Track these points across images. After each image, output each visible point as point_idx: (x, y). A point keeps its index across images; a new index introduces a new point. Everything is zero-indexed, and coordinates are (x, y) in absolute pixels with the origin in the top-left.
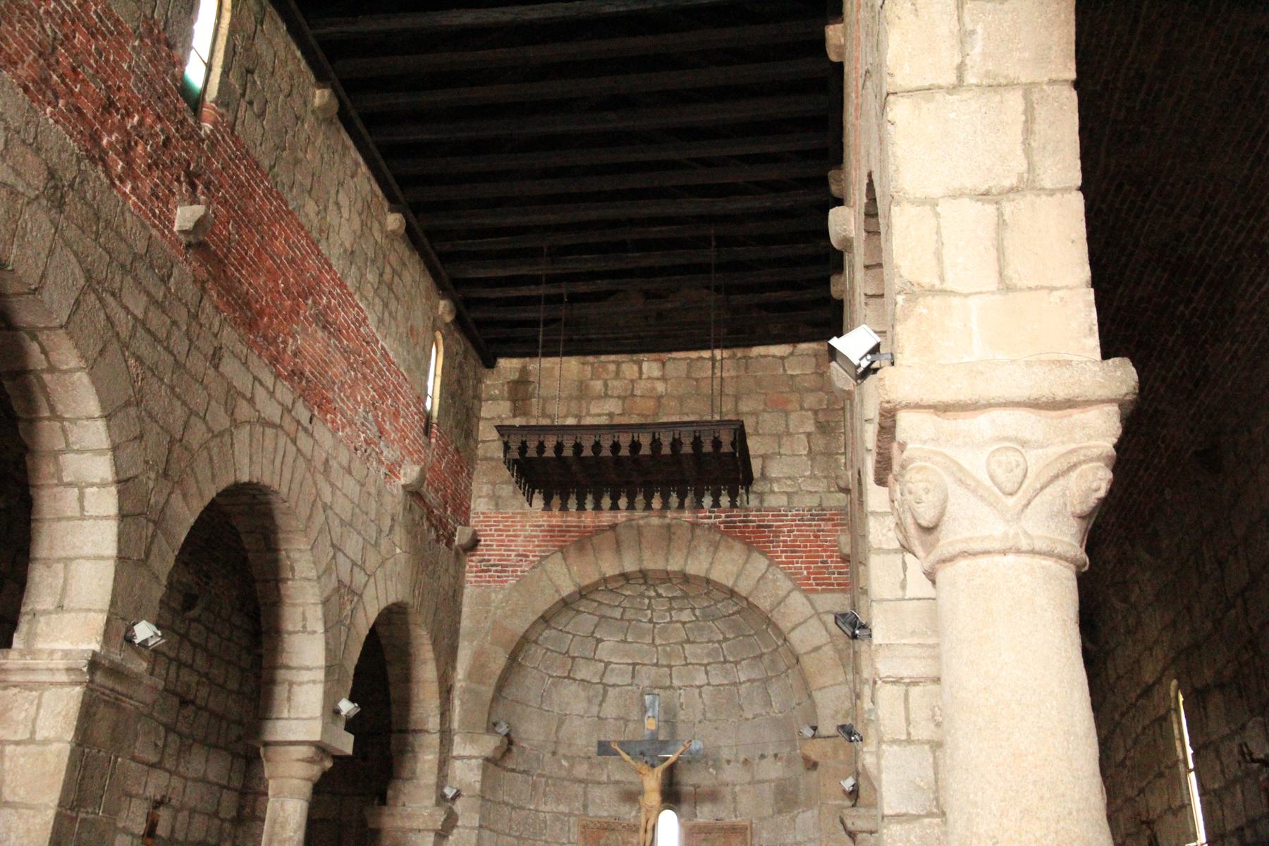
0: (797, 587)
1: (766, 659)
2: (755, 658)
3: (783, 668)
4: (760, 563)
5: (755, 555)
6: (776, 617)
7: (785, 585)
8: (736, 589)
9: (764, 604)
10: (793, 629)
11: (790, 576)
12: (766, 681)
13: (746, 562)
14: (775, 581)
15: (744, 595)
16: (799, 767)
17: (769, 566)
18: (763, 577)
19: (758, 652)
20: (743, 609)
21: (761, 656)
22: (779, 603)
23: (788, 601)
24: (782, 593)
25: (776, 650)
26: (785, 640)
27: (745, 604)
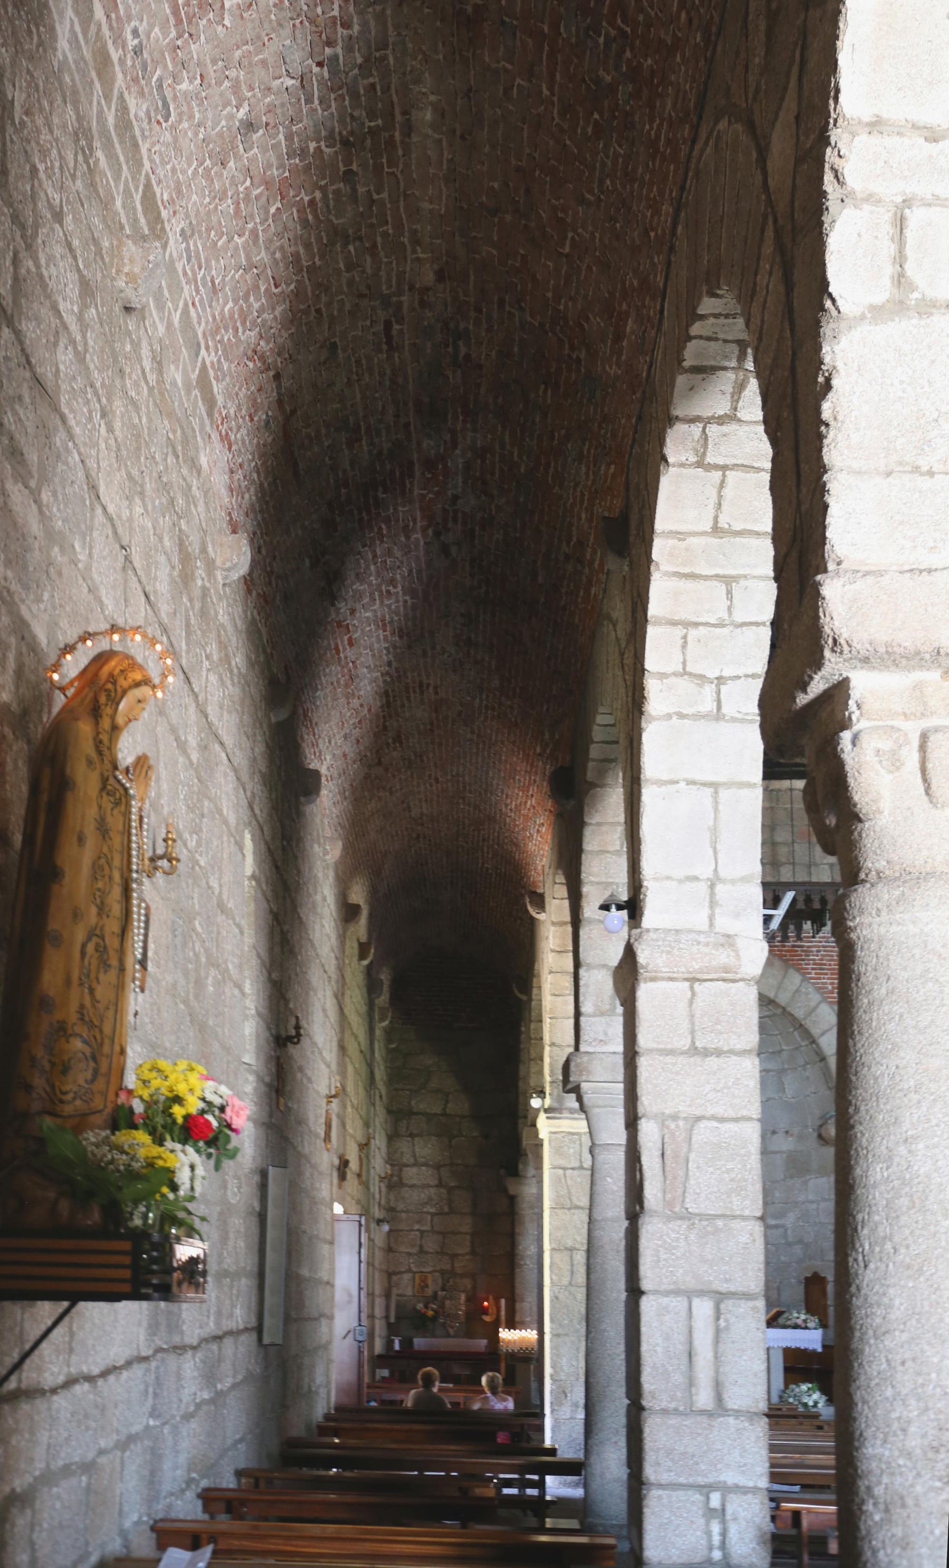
0: (824, 1000)
1: (785, 1055)
2: (773, 1053)
3: (801, 1061)
4: (795, 979)
5: (791, 971)
6: (808, 1024)
7: (815, 997)
8: (777, 1000)
9: (799, 1013)
10: (823, 1034)
11: (818, 990)
12: (781, 1072)
13: (784, 977)
14: (807, 994)
15: (783, 1004)
16: (813, 1141)
17: (802, 981)
18: (797, 991)
19: (778, 1048)
20: (774, 1015)
21: (781, 1051)
22: (810, 1014)
23: (819, 1011)
24: (813, 1004)
25: (797, 1048)
26: (814, 1042)
27: (779, 1011)
